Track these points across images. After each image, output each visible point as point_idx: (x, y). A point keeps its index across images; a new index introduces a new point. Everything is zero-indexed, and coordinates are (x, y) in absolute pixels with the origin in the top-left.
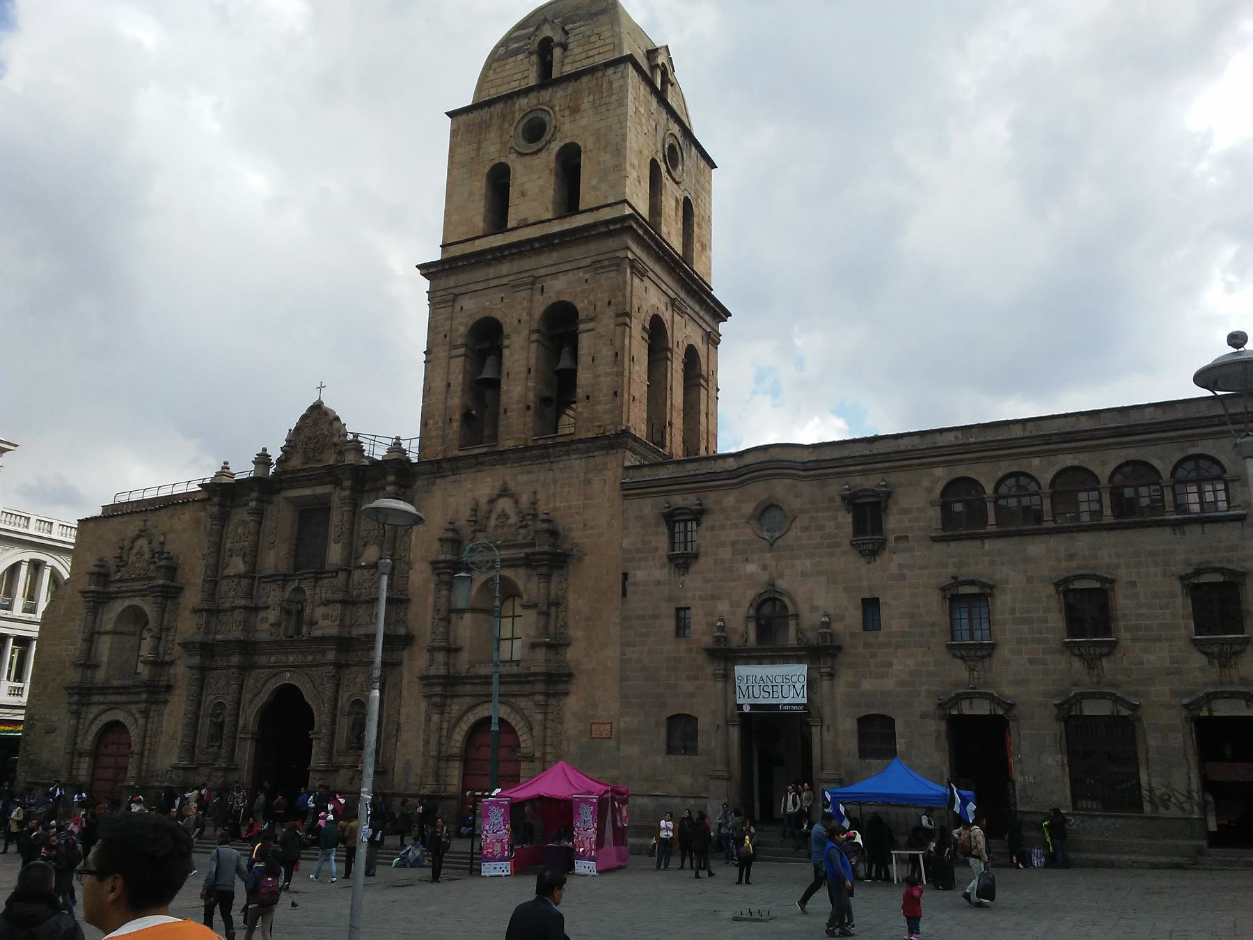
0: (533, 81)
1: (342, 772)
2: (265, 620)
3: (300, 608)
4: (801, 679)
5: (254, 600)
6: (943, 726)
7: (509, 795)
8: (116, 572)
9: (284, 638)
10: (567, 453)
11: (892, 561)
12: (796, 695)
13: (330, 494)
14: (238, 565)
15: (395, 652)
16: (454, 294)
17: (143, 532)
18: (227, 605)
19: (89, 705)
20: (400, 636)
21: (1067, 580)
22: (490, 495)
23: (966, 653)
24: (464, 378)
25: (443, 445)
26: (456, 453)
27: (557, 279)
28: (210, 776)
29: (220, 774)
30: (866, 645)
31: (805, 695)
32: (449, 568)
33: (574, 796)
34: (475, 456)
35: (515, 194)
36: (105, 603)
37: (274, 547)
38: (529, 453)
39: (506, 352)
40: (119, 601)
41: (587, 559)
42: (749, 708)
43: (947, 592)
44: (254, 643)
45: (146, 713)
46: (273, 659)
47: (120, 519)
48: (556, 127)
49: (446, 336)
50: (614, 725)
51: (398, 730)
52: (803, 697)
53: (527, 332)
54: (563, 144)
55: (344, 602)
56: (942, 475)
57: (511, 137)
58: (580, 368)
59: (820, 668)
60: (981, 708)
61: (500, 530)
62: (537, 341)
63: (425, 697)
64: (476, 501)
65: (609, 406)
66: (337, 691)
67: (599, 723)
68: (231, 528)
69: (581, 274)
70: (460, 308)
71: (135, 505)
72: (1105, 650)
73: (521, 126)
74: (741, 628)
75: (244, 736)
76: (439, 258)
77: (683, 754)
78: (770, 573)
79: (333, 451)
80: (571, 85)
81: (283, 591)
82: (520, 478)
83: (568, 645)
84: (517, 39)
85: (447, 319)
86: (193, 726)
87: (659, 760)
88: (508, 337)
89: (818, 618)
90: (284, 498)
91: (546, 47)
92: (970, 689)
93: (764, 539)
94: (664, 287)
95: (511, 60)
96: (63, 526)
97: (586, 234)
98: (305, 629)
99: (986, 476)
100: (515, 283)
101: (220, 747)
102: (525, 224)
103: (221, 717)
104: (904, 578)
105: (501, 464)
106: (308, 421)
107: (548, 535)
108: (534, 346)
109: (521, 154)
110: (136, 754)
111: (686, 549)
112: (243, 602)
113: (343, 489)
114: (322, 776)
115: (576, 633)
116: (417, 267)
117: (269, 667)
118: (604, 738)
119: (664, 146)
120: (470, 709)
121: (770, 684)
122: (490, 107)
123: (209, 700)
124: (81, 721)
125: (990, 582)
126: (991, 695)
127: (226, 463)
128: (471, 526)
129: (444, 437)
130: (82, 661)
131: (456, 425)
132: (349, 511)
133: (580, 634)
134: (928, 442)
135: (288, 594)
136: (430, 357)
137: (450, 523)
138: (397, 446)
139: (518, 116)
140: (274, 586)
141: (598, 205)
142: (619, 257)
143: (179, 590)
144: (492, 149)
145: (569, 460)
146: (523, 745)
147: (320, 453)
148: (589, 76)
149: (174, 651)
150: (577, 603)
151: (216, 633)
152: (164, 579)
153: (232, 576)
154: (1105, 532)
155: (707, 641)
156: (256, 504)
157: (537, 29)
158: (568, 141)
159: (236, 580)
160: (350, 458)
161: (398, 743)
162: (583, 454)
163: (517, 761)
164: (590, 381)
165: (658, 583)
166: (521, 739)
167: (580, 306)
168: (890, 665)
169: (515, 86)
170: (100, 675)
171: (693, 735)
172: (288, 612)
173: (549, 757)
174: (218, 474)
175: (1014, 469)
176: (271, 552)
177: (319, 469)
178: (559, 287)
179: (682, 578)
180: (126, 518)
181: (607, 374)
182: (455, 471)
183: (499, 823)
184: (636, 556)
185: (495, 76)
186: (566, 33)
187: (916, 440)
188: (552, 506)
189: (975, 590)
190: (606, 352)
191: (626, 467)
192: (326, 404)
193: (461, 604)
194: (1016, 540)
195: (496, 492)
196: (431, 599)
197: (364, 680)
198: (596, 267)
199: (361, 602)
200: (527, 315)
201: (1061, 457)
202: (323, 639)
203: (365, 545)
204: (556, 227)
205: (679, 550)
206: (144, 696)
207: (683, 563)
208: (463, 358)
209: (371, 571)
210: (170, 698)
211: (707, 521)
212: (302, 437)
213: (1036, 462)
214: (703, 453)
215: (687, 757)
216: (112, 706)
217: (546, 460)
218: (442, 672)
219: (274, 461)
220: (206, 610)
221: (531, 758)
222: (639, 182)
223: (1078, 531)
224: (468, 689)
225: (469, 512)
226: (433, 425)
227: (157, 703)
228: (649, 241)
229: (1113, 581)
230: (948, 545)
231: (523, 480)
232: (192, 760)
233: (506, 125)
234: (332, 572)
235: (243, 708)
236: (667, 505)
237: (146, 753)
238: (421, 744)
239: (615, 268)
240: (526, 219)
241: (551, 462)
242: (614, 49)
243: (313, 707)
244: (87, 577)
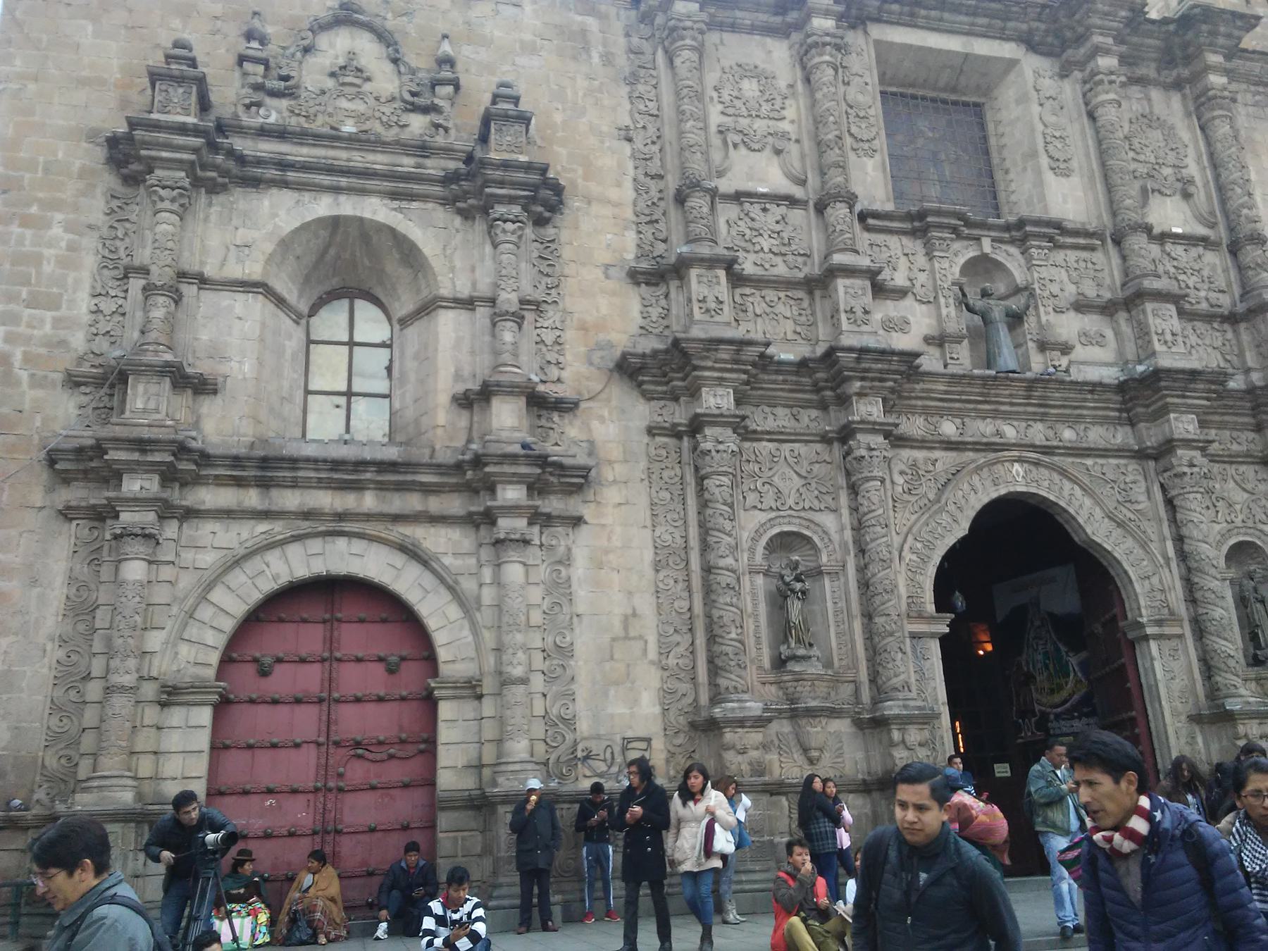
13: (1012, 64)
36: (214, 189)
40: (288, 197)
90: (877, 43)
117: (950, 445)
140: (905, 240)
153: (763, 196)
209: (1194, 252)
210: (587, 512)
216: (305, 526)
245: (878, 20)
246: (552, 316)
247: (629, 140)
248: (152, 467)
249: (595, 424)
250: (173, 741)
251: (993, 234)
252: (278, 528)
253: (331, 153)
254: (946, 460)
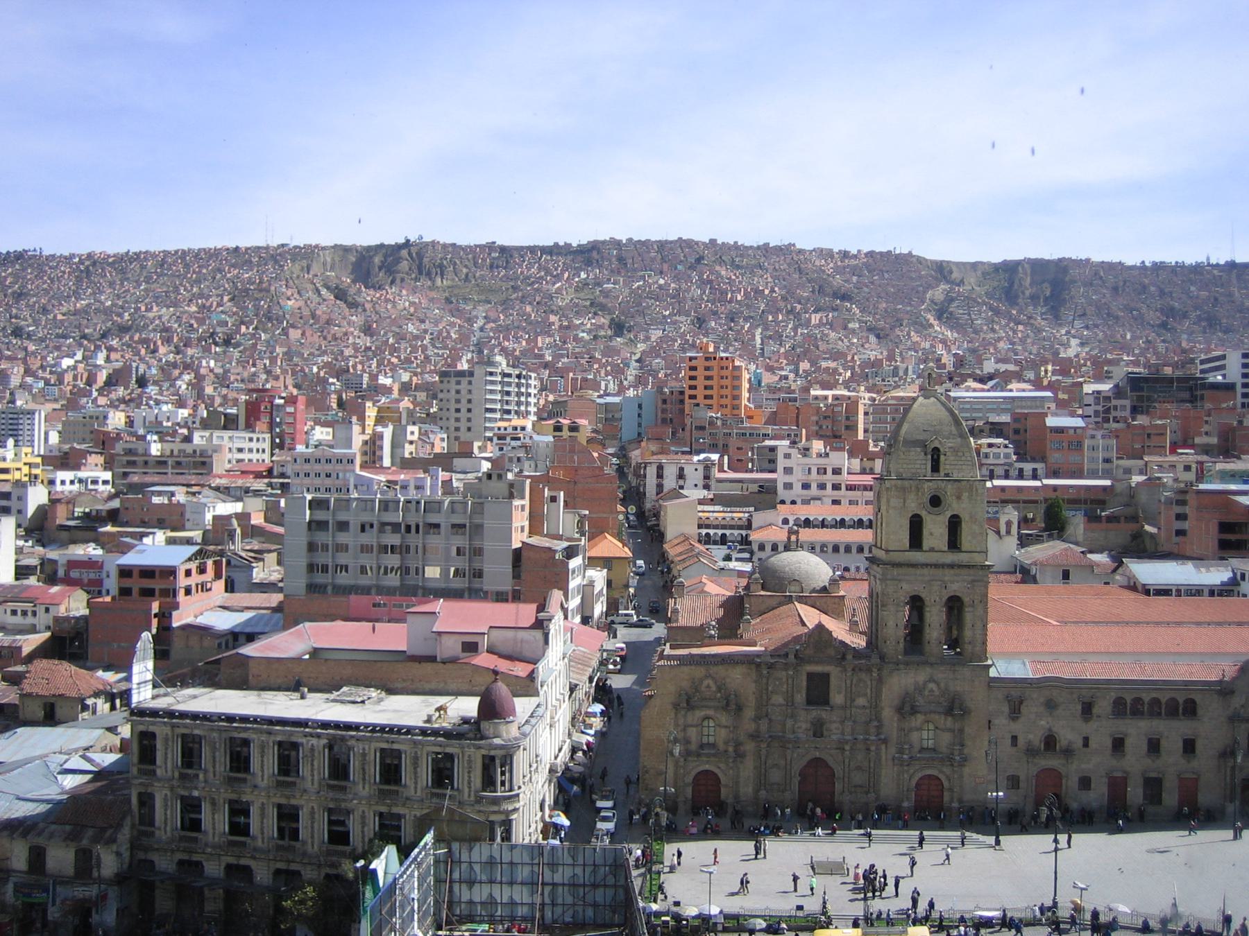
11: (1093, 725)
53: (938, 607)
56: (1113, 695)
60: (1119, 774)
102: (932, 550)
131: (902, 645)
144: (913, 505)
167: (966, 600)
178: (956, 588)
196: (895, 725)
231: (942, 674)
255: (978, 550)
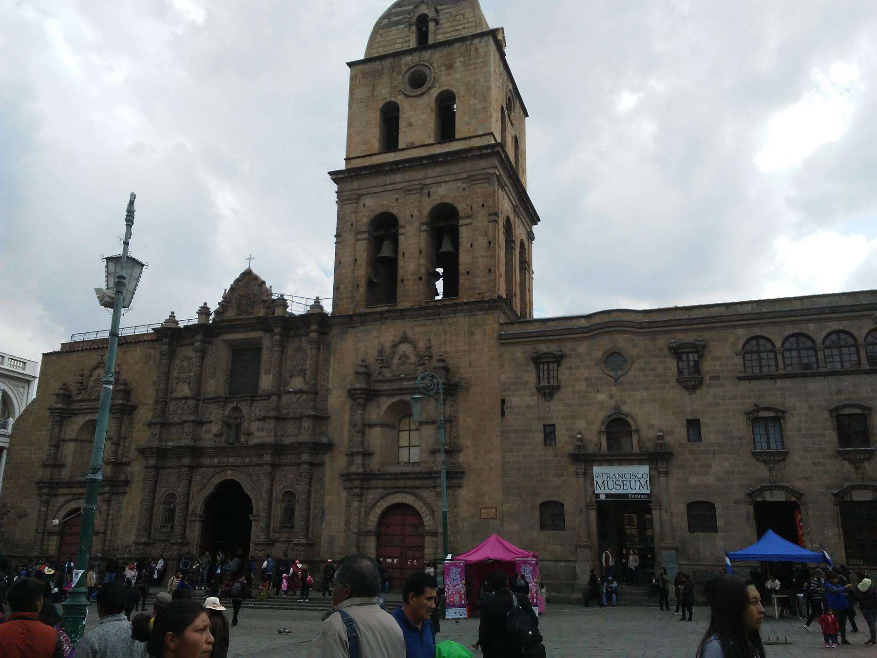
0: (413, 44)
1: (278, 545)
2: (209, 431)
3: (239, 422)
4: (645, 476)
5: (200, 416)
6: (751, 509)
7: (464, 559)
8: (79, 394)
9: (226, 445)
10: (455, 312)
11: (708, 394)
12: (641, 488)
13: (261, 338)
14: (184, 390)
15: (319, 456)
16: (358, 194)
17: (101, 364)
18: (176, 419)
19: (56, 495)
20: (324, 444)
21: (837, 408)
22: (393, 341)
23: (767, 458)
24: (368, 256)
25: (352, 304)
26: (363, 310)
27: (441, 187)
28: (164, 550)
29: (175, 547)
30: (691, 452)
31: (649, 488)
32: (364, 394)
33: (516, 559)
34: (381, 313)
35: (404, 124)
36: (68, 417)
37: (215, 377)
38: (423, 312)
39: (401, 238)
40: (81, 416)
41: (472, 389)
42: (604, 496)
43: (751, 416)
44: (201, 449)
45: (108, 502)
46: (216, 461)
47: (80, 354)
48: (435, 78)
49: (352, 225)
50: (499, 509)
51: (323, 512)
52: (647, 488)
53: (417, 224)
54: (441, 90)
55: (278, 419)
56: (742, 333)
57: (400, 83)
58: (461, 251)
59: (658, 469)
60: (779, 497)
61: (402, 367)
62: (426, 231)
63: (345, 489)
64: (382, 346)
65: (485, 279)
66: (272, 485)
67: (486, 508)
68: (177, 362)
69: (460, 184)
70: (363, 205)
71: (90, 343)
72: (867, 456)
73: (407, 76)
74: (595, 440)
75: (192, 519)
76: (344, 168)
77: (553, 530)
78: (616, 401)
79: (262, 306)
80: (447, 47)
81: (224, 410)
82: (417, 329)
83: (460, 451)
84: (397, 14)
85: (352, 212)
86: (151, 510)
87: (535, 534)
88: (403, 227)
89: (652, 434)
90: (223, 340)
91: (423, 21)
92: (772, 483)
93: (611, 376)
94: (511, 197)
95: (394, 28)
96: (12, 359)
97: (464, 156)
98: (243, 439)
99: (776, 335)
100: (408, 188)
101: (172, 527)
102: (412, 146)
103: (172, 504)
104: (717, 405)
105: (400, 319)
106: (240, 283)
107: (444, 371)
108: (423, 235)
109: (408, 96)
110: (101, 533)
111: (549, 382)
112: (192, 418)
113: (275, 335)
114: (263, 548)
115: (466, 442)
116: (330, 173)
118: (490, 519)
119: (506, 98)
120: (383, 498)
121: (620, 479)
122: (382, 61)
123: (162, 491)
124: (51, 508)
125: (783, 409)
126: (787, 487)
127: (173, 313)
128: (379, 363)
129: (353, 298)
130: (51, 462)
131: (362, 290)
132: (199, 357)
133: (469, 443)
134: (732, 311)
135: (228, 411)
136: (340, 240)
137: (362, 361)
138: (318, 303)
139: (404, 69)
140: (215, 406)
141: (470, 135)
142: (490, 173)
143: (134, 408)
145: (455, 317)
146: (426, 524)
147: (252, 308)
148: (460, 44)
149: (130, 454)
150: (466, 420)
151: (167, 441)
152: (122, 400)
154: (864, 375)
155: (570, 449)
156: (201, 345)
157: (416, 7)
158: (444, 88)
159: (183, 401)
160: (279, 312)
161: (323, 524)
162: (466, 313)
163: (422, 536)
164: (469, 261)
165: (529, 407)
166: (424, 520)
167: (461, 207)
168: (710, 466)
169: (398, 47)
170: (65, 474)
171: (562, 516)
172: (229, 426)
173: (449, 533)
174: (167, 321)
175: (796, 331)
176: (212, 381)
177: (251, 319)
178: (444, 193)
179: (548, 404)
180: (85, 353)
181: (483, 257)
182: (363, 323)
183: (529, 577)
184: (512, 387)
185: (382, 39)
186: (437, 12)
187: (723, 309)
188: (443, 350)
189: (772, 414)
190: (482, 241)
191: (501, 323)
192: (256, 271)
193: (374, 422)
194: (799, 380)
195: (397, 339)
196: (347, 417)
197: (293, 476)
198: (471, 179)
199: (291, 419)
200: (418, 212)
201: (829, 324)
202: (262, 446)
203: (291, 376)
204: (438, 150)
205: (544, 383)
206: (107, 489)
207: (549, 393)
208: (366, 242)
209: (297, 396)
211: (565, 364)
212: (235, 296)
213: (812, 326)
214: (528, 317)
215: (557, 532)
217: (437, 317)
218: (361, 470)
219: (212, 310)
220: (160, 423)
221: (434, 534)
222: (497, 121)
223: (844, 375)
224: (380, 483)
225: (375, 353)
226: (344, 288)
227: (117, 494)
228: (506, 163)
229: (870, 409)
230: (750, 382)
231: (418, 331)
232: (149, 537)
233: (395, 74)
234: (265, 396)
235: (192, 498)
236: (559, 349)
237: (109, 532)
238: (343, 524)
239: (487, 181)
240: (413, 143)
241: (441, 319)
242: (476, 26)
243: (251, 496)
244: (55, 397)
245: (223, 334)
246: (129, 440)
247: (155, 385)
248: (46, 487)
249: (134, 467)
250: (51, 543)
251: (237, 400)
252: (71, 497)
253: (93, 403)
254: (211, 469)
255: (480, 132)
